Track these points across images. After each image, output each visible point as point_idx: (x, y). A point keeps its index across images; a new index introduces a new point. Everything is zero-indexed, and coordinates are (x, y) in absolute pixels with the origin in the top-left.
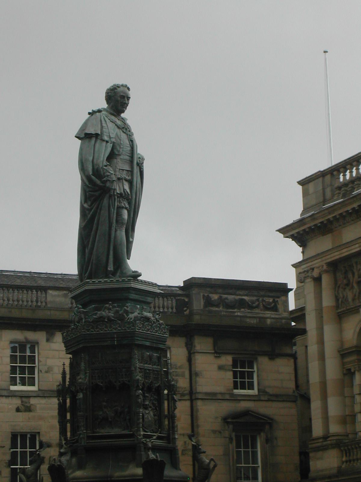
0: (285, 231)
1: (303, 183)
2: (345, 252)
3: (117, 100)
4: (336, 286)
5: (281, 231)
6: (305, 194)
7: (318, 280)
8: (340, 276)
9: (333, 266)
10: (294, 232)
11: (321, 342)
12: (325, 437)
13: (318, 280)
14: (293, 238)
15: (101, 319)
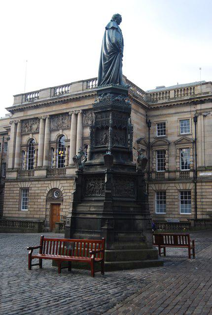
0: (7, 109)
1: (15, 96)
2: (28, 118)
3: (117, 19)
4: (22, 127)
5: (6, 108)
6: (15, 100)
7: (16, 124)
8: (24, 125)
9: (22, 121)
10: (11, 109)
11: (15, 142)
12: (13, 169)
13: (16, 124)
14: (10, 111)
15: (118, 100)
